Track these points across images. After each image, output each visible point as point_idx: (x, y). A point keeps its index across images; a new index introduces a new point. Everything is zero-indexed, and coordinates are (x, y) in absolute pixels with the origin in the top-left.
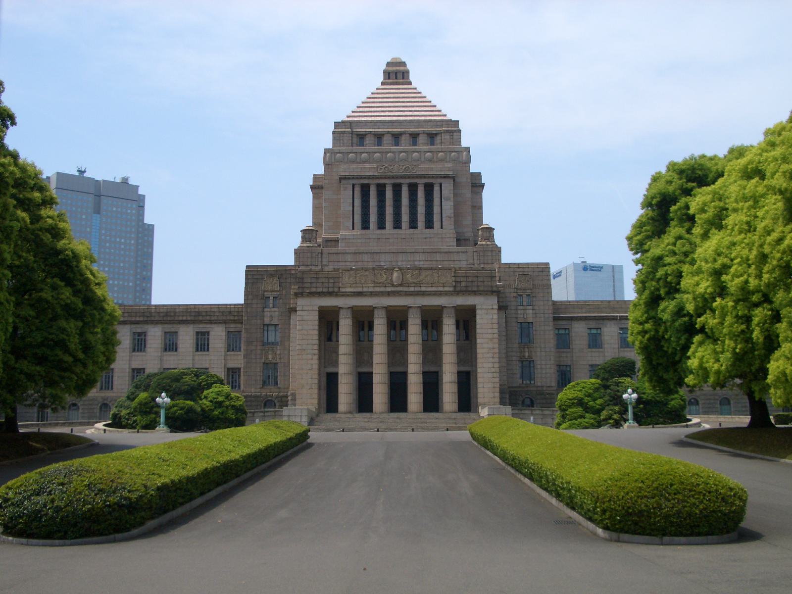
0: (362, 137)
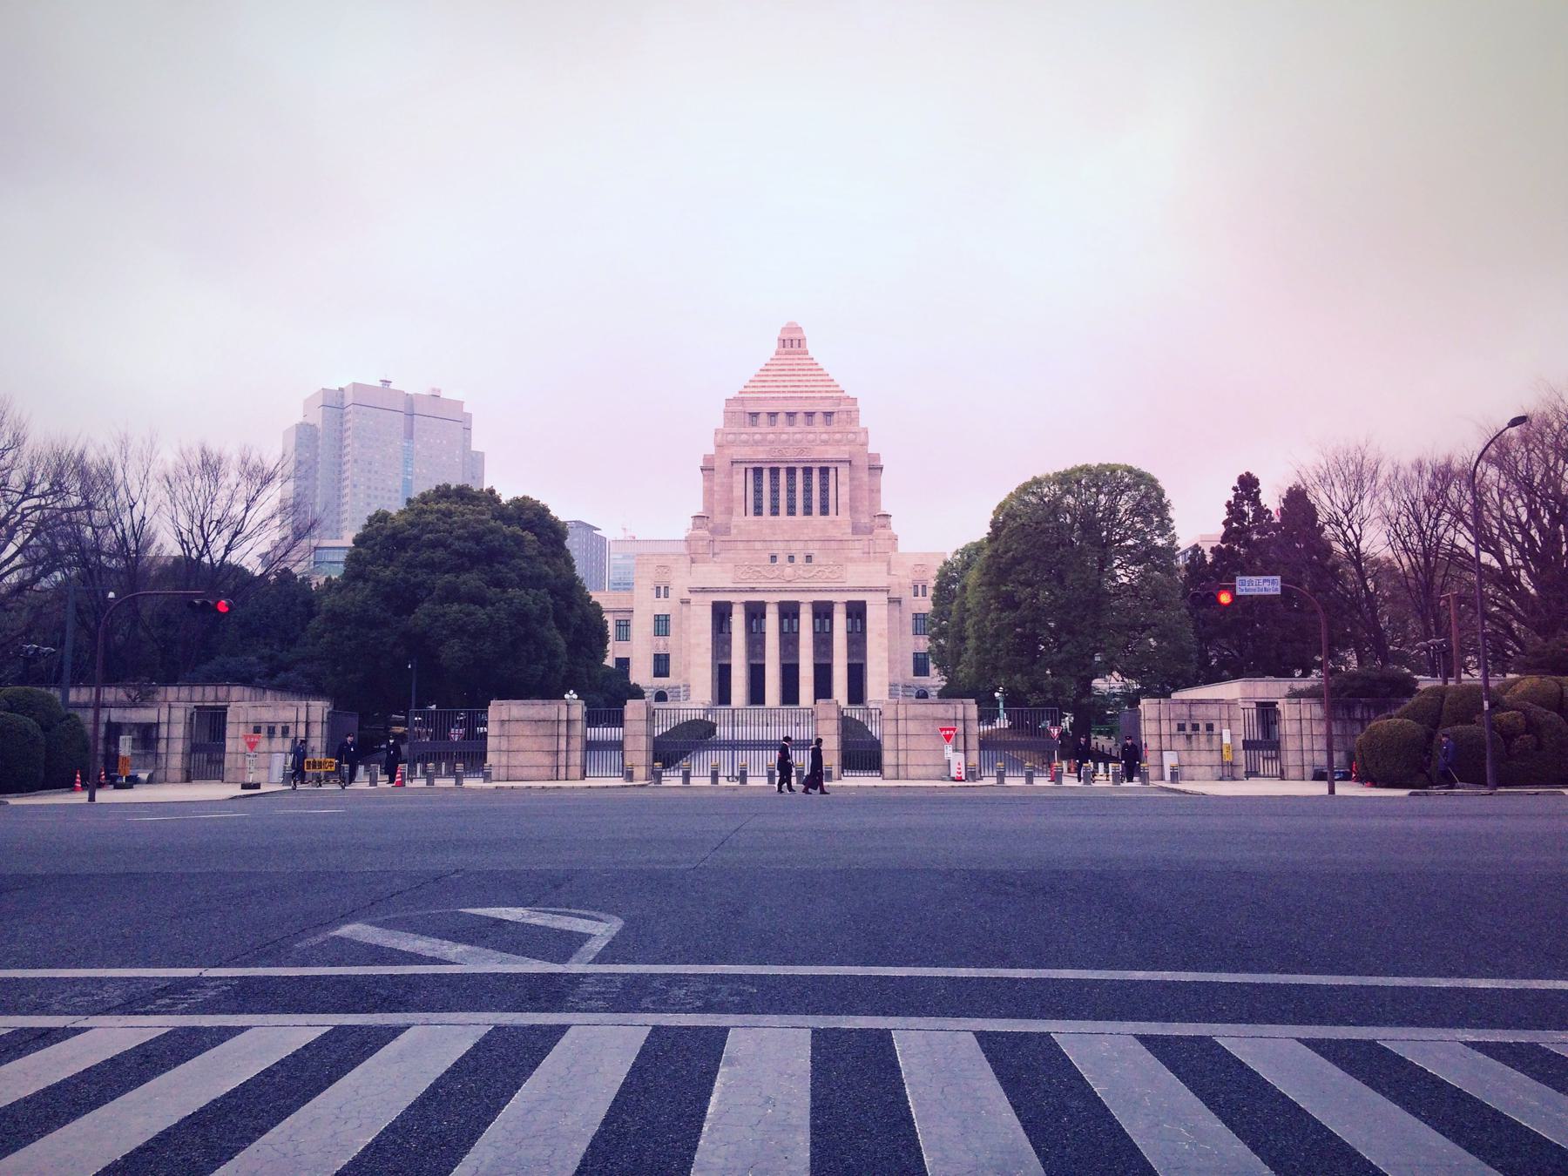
0: (755, 415)
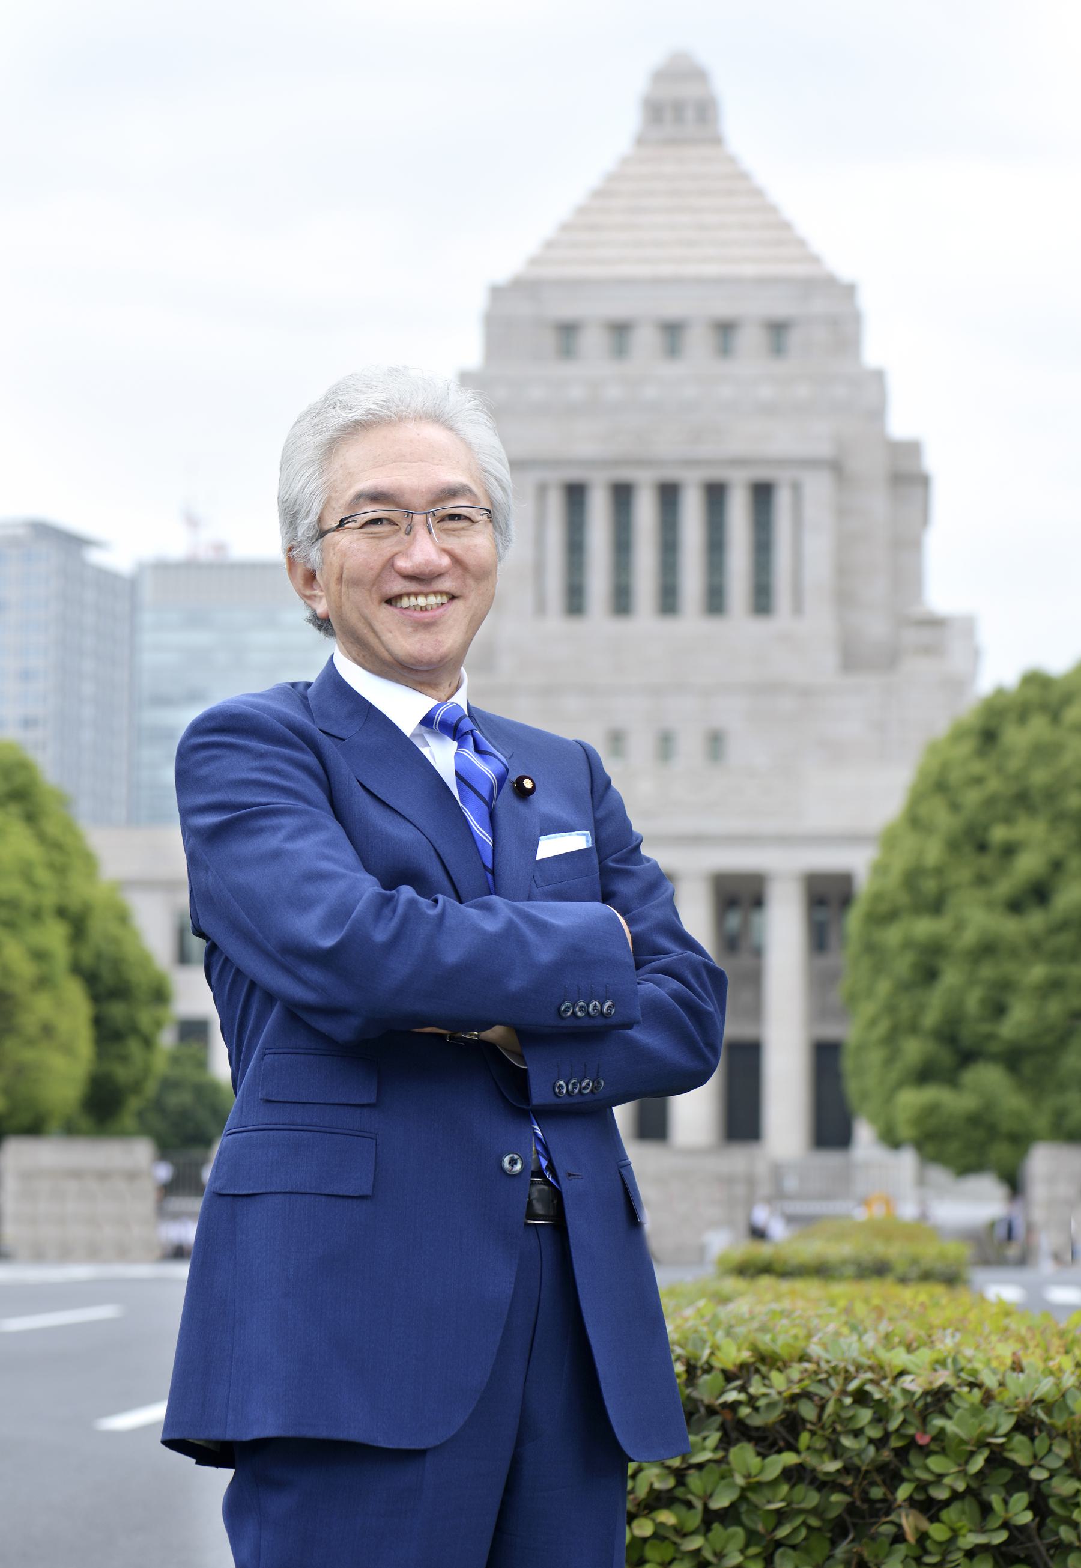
0: (567, 332)
